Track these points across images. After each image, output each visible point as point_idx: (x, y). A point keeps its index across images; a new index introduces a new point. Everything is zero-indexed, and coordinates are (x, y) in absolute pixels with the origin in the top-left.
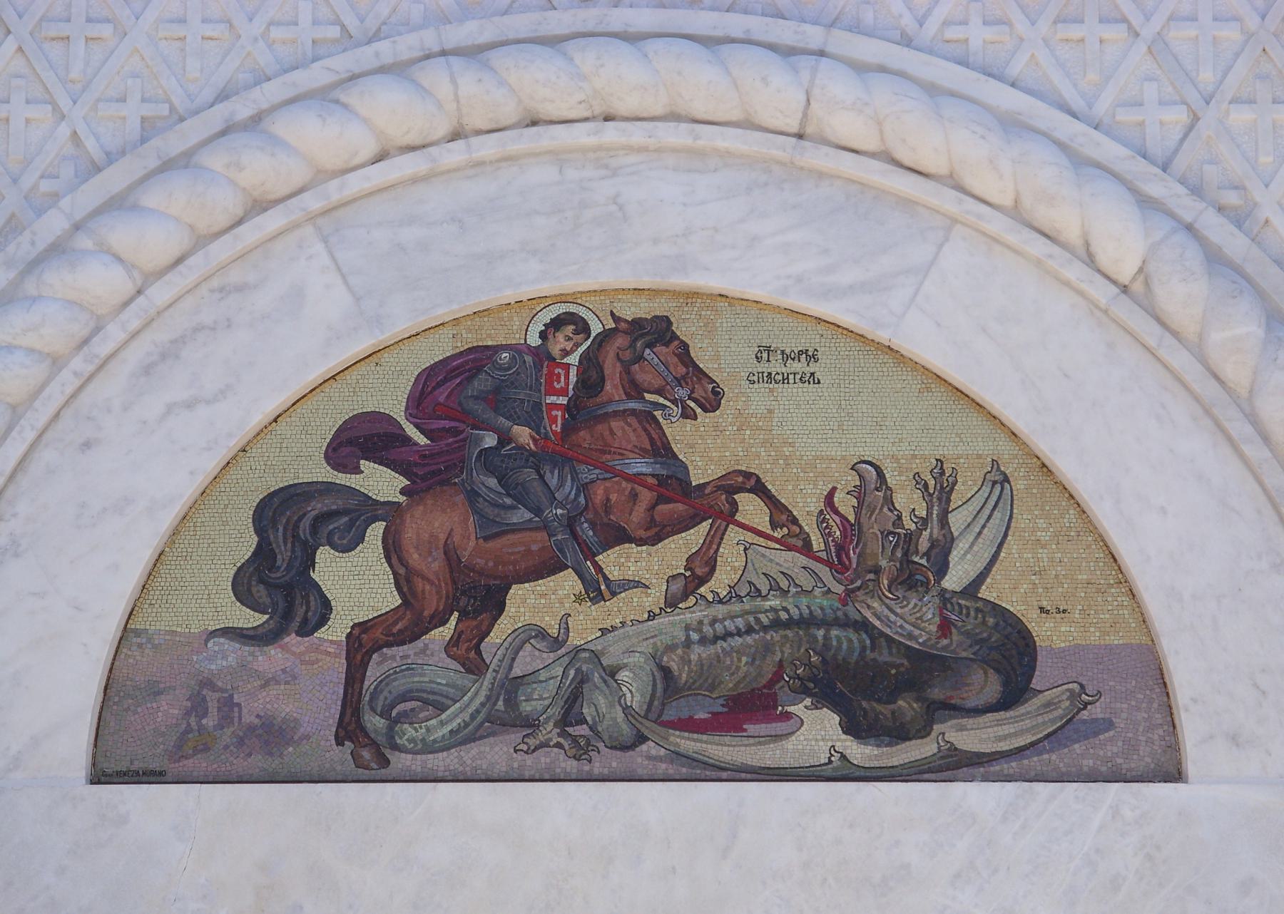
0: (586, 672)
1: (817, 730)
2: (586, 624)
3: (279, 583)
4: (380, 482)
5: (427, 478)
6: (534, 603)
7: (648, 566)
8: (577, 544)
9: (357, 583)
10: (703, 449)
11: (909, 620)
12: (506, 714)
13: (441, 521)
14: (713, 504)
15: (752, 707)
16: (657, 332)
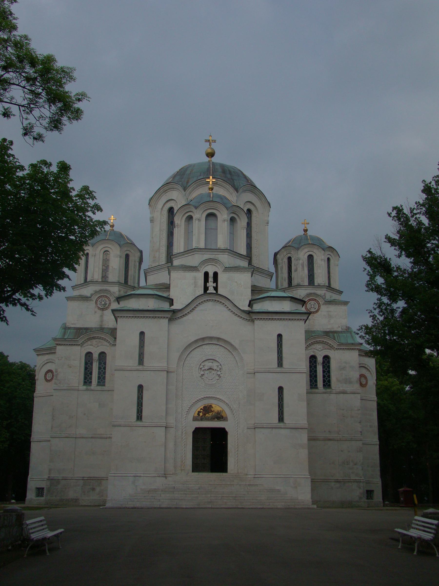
0: (209, 417)
1: (216, 420)
2: (209, 416)
3: (198, 414)
4: (202, 411)
5: (203, 410)
6: (207, 415)
7: (211, 414)
8: (208, 413)
9: (201, 414)
10: (213, 410)
11: (219, 416)
12: (206, 419)
13: (204, 412)
14: (213, 411)
15: (214, 419)
16: (211, 405)
